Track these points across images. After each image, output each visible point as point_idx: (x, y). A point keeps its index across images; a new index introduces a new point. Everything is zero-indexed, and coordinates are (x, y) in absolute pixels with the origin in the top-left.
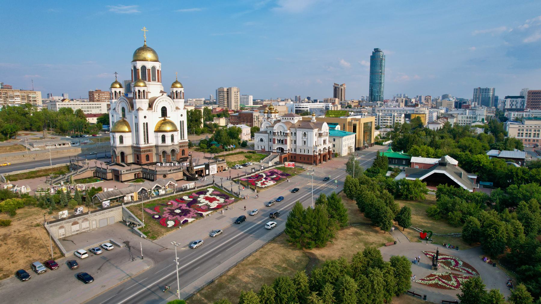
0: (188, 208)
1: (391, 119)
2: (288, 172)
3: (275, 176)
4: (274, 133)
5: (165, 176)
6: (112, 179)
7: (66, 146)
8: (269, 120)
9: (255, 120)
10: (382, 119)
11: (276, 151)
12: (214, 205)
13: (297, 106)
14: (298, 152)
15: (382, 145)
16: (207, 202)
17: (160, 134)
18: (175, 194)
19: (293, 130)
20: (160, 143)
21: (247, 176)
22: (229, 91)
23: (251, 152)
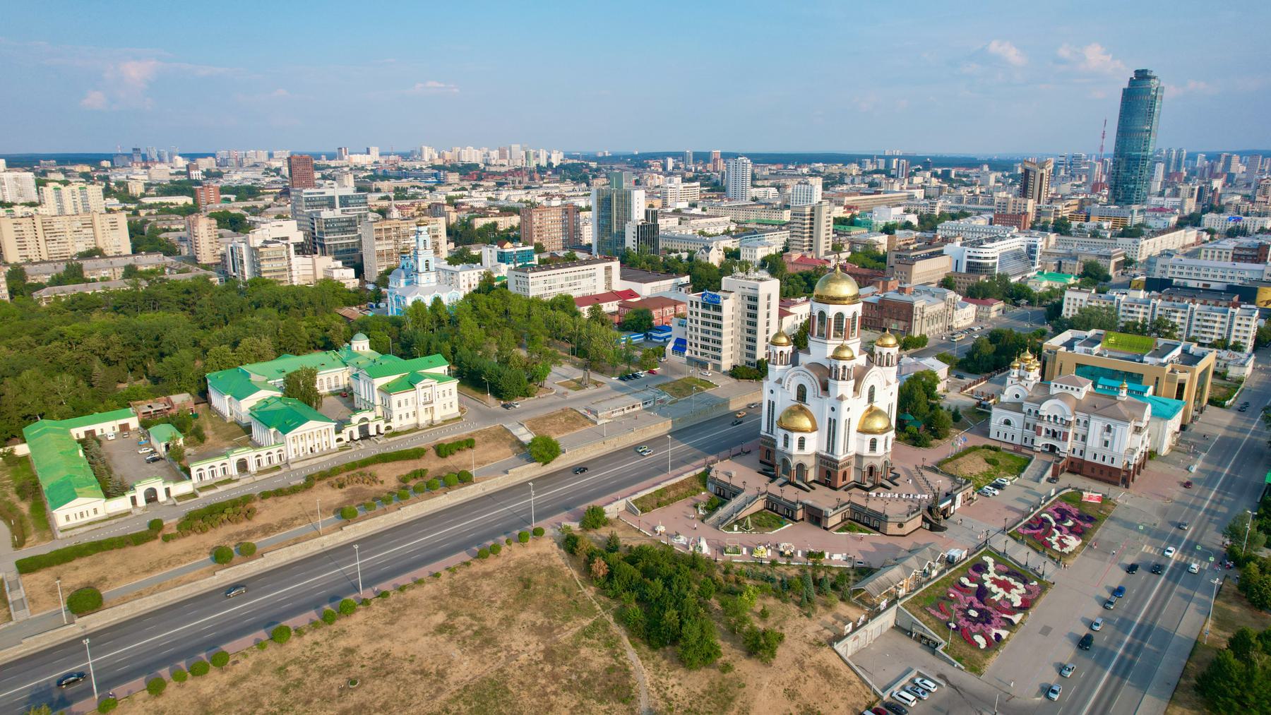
0: (983, 606)
1: (1223, 320)
2: (1093, 513)
3: (1070, 523)
4: (1040, 418)
5: (901, 525)
6: (803, 519)
7: (637, 409)
8: (1023, 383)
9: (918, 317)
10: (1199, 317)
11: (1039, 450)
12: (1016, 600)
13: (971, 254)
14: (1088, 457)
15: (1222, 406)
16: (1002, 592)
17: (869, 437)
18: (947, 573)
19: (1082, 417)
20: (866, 451)
21: (1025, 521)
22: (816, 213)
23: (990, 448)
